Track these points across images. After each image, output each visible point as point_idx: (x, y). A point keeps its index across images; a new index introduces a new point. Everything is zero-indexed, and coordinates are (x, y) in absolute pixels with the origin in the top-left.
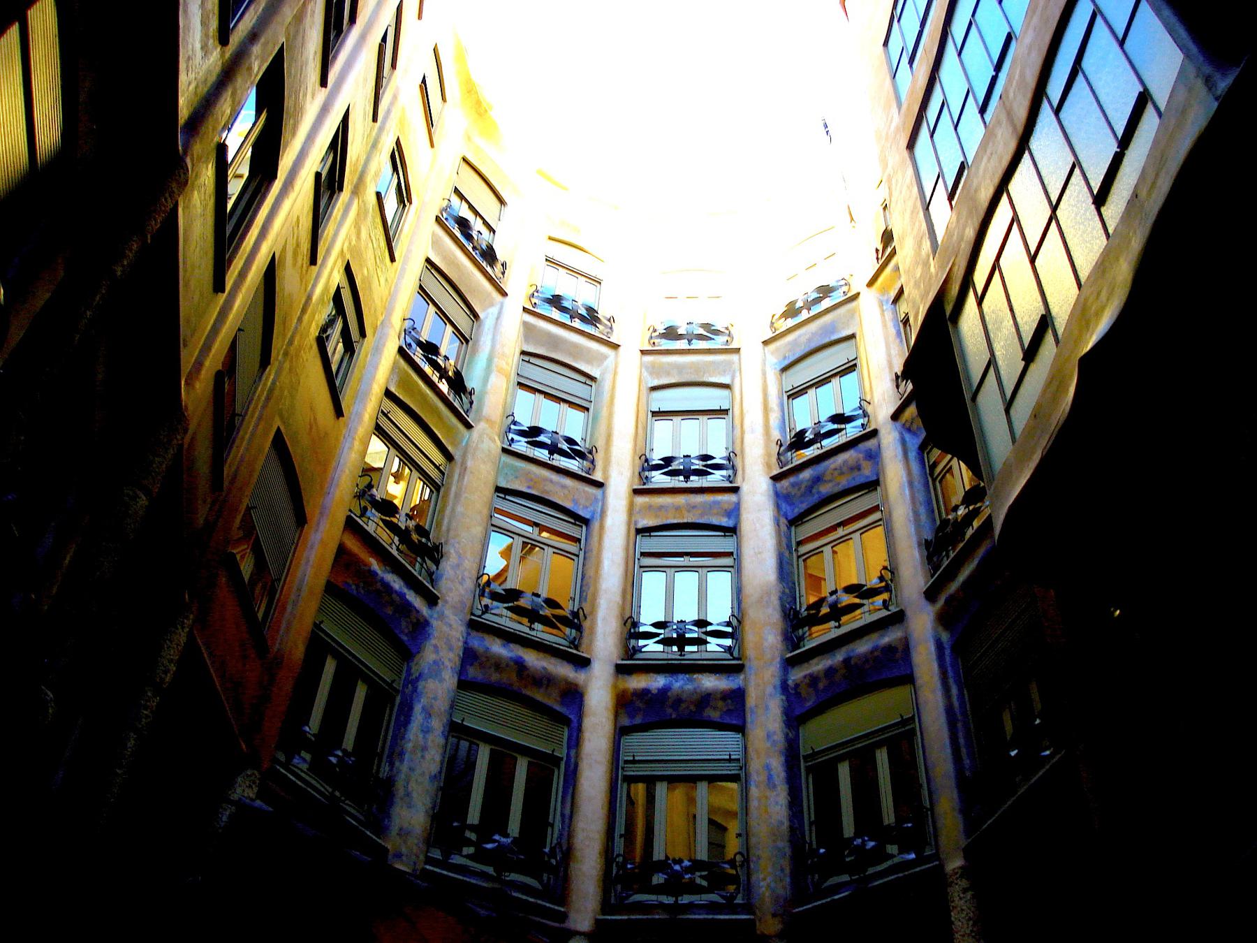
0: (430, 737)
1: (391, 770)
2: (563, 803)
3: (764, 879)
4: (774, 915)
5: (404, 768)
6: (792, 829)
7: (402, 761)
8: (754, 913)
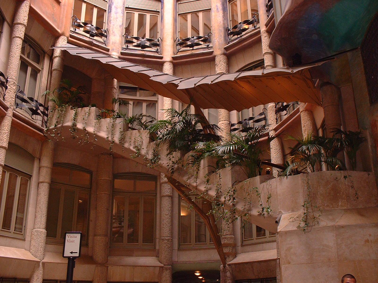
0: (118, 15)
1: (108, 26)
2: (161, 26)
3: (216, 39)
4: (219, 49)
5: (112, 25)
6: (224, 24)
7: (110, 23)
8: (214, 49)
